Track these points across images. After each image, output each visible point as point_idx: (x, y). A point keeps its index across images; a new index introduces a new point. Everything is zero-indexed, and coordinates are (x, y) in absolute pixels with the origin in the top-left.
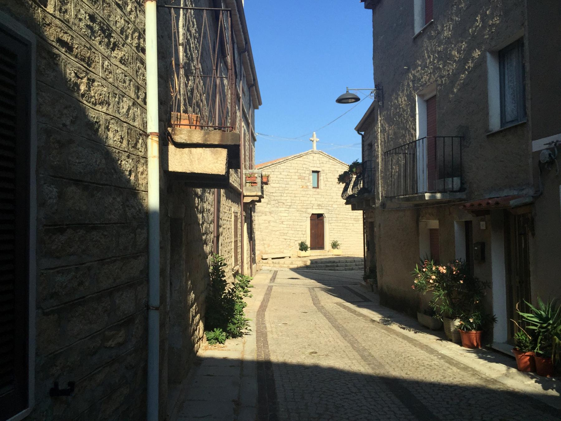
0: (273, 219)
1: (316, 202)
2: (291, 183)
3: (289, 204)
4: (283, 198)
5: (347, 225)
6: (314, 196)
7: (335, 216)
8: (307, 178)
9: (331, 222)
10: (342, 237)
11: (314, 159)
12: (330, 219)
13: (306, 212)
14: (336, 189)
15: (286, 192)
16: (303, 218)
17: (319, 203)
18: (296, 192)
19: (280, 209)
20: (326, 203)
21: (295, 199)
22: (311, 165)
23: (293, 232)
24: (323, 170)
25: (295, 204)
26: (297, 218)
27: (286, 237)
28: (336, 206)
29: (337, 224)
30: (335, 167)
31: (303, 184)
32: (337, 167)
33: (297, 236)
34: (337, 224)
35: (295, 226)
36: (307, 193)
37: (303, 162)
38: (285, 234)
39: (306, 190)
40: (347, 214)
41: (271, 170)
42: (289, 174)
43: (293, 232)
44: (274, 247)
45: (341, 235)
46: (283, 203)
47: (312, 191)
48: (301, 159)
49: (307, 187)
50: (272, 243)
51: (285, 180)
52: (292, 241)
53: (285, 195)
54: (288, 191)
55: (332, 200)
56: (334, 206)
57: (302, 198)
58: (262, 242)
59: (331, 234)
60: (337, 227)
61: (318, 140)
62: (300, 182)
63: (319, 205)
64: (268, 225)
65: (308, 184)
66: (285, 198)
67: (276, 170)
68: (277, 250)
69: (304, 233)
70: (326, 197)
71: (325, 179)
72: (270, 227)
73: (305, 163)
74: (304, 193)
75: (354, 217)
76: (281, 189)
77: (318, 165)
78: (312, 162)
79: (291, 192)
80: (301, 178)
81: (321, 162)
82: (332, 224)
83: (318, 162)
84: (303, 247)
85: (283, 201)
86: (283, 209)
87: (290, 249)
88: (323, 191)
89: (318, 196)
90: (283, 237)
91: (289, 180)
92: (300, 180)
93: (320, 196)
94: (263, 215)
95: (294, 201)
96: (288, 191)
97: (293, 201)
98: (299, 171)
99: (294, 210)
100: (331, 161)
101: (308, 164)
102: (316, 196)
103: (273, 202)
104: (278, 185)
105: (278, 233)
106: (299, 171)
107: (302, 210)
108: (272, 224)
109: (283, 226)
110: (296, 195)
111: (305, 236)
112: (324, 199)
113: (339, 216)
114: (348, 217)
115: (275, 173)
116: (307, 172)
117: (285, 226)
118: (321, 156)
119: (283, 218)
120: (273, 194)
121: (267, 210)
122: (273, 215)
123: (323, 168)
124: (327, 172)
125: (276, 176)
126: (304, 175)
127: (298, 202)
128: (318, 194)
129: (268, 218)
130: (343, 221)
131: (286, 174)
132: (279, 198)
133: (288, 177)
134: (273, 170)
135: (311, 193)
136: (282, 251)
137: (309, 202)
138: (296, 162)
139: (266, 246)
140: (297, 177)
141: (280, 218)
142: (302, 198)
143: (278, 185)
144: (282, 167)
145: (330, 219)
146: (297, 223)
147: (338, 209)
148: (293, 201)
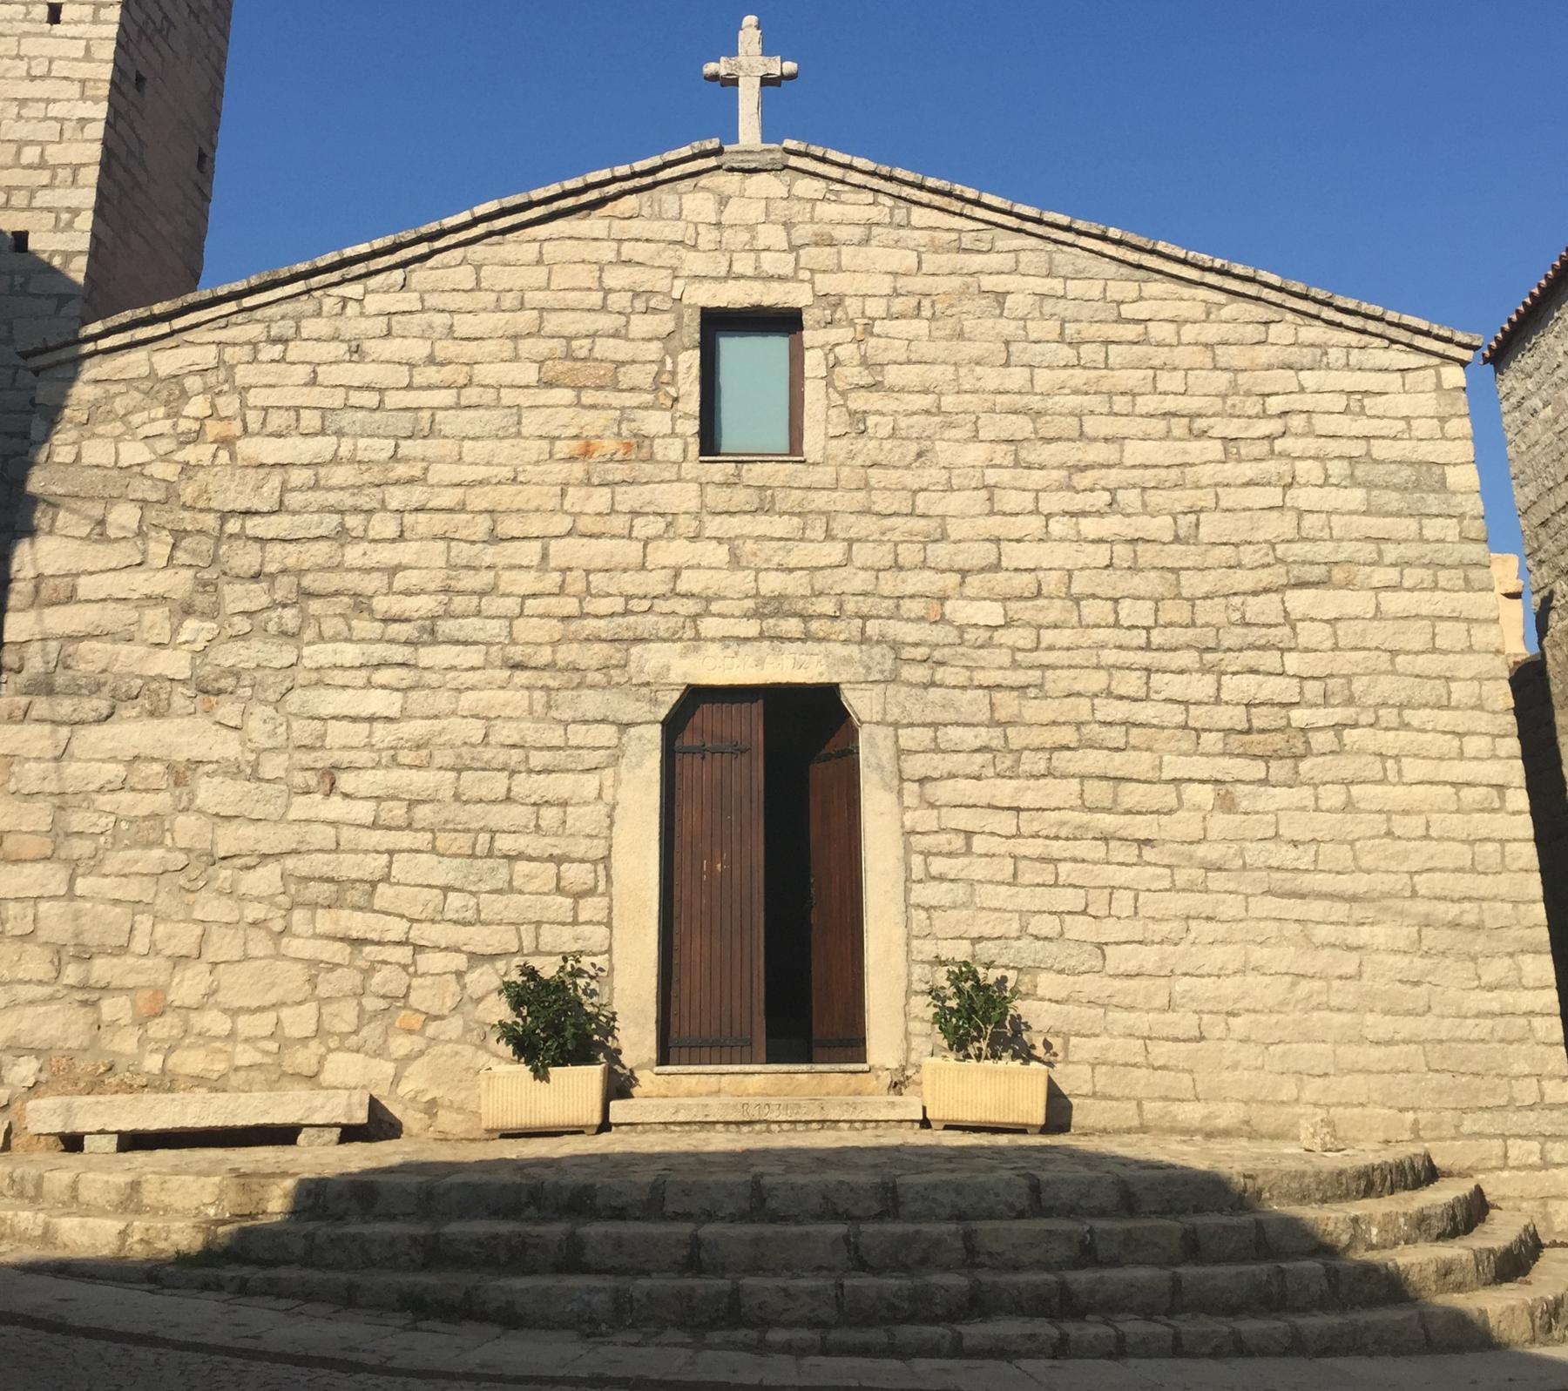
0: (229, 747)
1: (742, 581)
2: (452, 422)
3: (424, 605)
4: (353, 554)
5: (1132, 795)
6: (713, 526)
7: (973, 704)
8: (641, 376)
9: (917, 766)
10: (1079, 928)
11: (731, 214)
12: (908, 738)
13: (612, 676)
14: (976, 453)
15: (396, 498)
16: (578, 735)
17: (772, 583)
18: (505, 496)
19: (317, 654)
20: (860, 581)
21: (490, 554)
22: (694, 263)
23: (445, 872)
24: (836, 301)
25: (492, 605)
26: (505, 733)
27: (357, 923)
28: (992, 613)
29: (1005, 791)
30: (976, 261)
31: (593, 422)
32: (993, 261)
33: (493, 906)
34: (1005, 791)
35: (473, 815)
36: (629, 498)
37: (607, 252)
38: (341, 891)
39: (618, 472)
40: (1131, 683)
41: (255, 331)
42: (446, 349)
43: (445, 872)
44: (214, 1022)
45: (1070, 899)
46: (361, 604)
47: (683, 482)
48: (591, 225)
49: (638, 447)
50: (188, 986)
51: (393, 399)
52: (432, 962)
53: (384, 526)
54: (417, 495)
55: (940, 553)
56: (960, 611)
57: (562, 552)
58: (72, 973)
59: (921, 894)
60: (1006, 823)
61: (776, 67)
62: (556, 412)
63: (769, 607)
64: (161, 801)
65: (655, 422)
66: (386, 555)
67: (311, 327)
68: (245, 1056)
69: (577, 875)
70: (866, 526)
71: (851, 374)
72: (187, 828)
73: (628, 250)
74: (600, 499)
75: (1232, 716)
76: (341, 475)
77: (785, 263)
78: (707, 238)
79: (448, 498)
80: (572, 371)
81: (802, 233)
82: (943, 791)
83: (772, 235)
84: (552, 1024)
85: (353, 581)
86: (350, 653)
87: (401, 1045)
88: (824, 475)
89: (762, 525)
90: (325, 921)
91: (445, 397)
92: (568, 395)
93: (781, 526)
94: (127, 711)
95: (483, 579)
96: (417, 495)
97: (469, 581)
98: (553, 323)
99: (473, 656)
100: (919, 216)
101: (668, 256)
102: (735, 525)
103: (238, 597)
104: (323, 446)
105: (265, 879)
106: (553, 323)
107: (567, 654)
108: (210, 792)
109: (335, 808)
110: (510, 526)
111: (591, 908)
112: (835, 552)
113: (1034, 710)
114: (1145, 712)
115: (295, 351)
116: (641, 325)
117: (363, 811)
118: (805, 186)
119: (338, 733)
120: (255, 526)
121: (174, 663)
122: (228, 711)
123: (825, 283)
124: (875, 307)
125: (302, 373)
126: (608, 348)
127: (526, 582)
128: (763, 509)
129: (186, 735)
130: (1094, 761)
131: (420, 350)
132: (320, 552)
133: (432, 374)
134: (287, 328)
135: (682, 497)
136: (303, 1059)
137: (655, 582)
138: (531, 251)
139: (113, 1008)
140: (529, 374)
141: (303, 731)
142: (562, 552)
143: (323, 446)
144: (373, 303)
145: (908, 738)
146: (499, 783)
147: (1021, 637)
148: (469, 581)
